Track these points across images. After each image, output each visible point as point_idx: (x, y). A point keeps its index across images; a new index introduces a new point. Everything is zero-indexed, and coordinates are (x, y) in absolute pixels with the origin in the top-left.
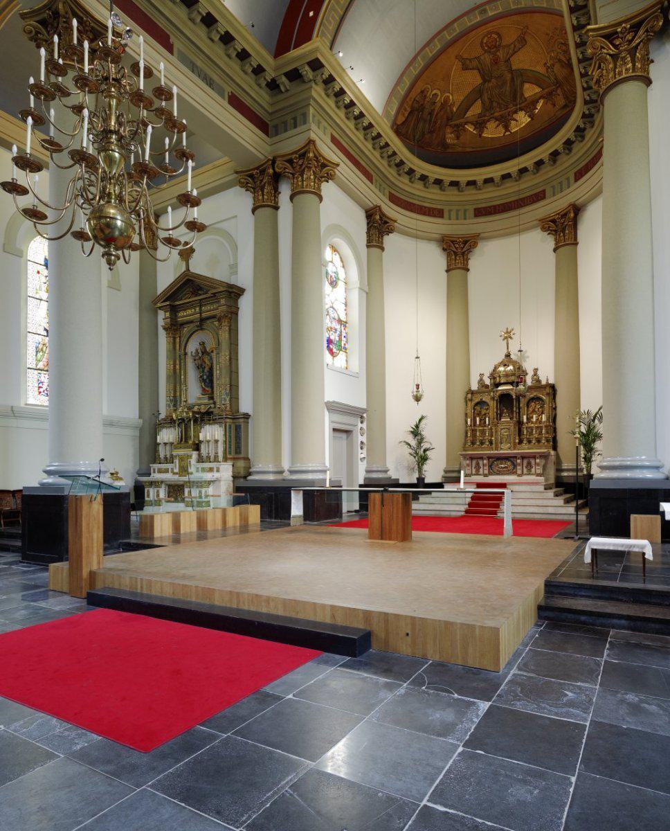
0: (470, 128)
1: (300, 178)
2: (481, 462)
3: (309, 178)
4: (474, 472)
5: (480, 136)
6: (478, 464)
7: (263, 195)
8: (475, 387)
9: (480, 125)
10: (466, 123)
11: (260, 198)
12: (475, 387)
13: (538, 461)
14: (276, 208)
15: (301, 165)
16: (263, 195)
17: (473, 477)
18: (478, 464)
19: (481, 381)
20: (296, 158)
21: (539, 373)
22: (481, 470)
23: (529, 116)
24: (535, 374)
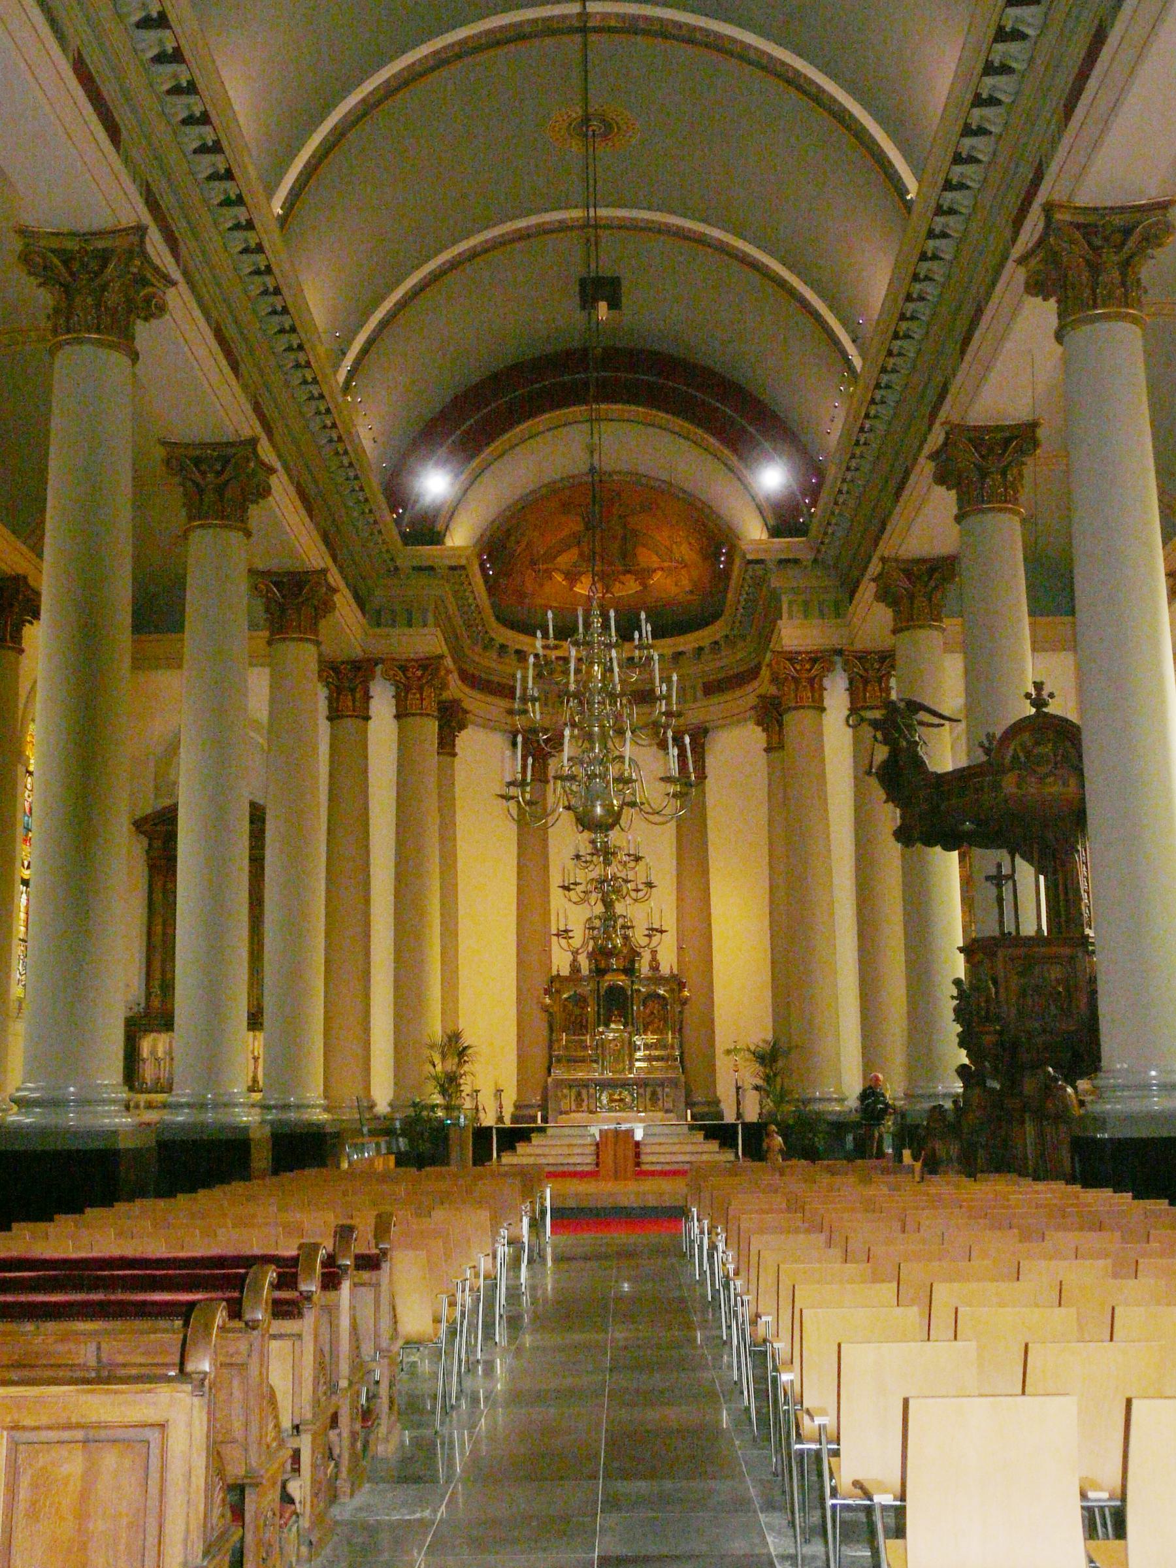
0: (559, 578)
1: (418, 696)
2: (584, 1092)
3: (429, 696)
4: (573, 1107)
5: (571, 589)
6: (579, 1094)
7: (354, 700)
8: (565, 972)
9: (572, 577)
10: (554, 570)
11: (350, 704)
12: (565, 972)
13: (667, 1090)
14: (367, 718)
15: (419, 678)
16: (354, 700)
17: (573, 1115)
18: (579, 1094)
19: (575, 968)
20: (413, 667)
21: (659, 957)
22: (585, 1104)
23: (640, 584)
24: (654, 959)
